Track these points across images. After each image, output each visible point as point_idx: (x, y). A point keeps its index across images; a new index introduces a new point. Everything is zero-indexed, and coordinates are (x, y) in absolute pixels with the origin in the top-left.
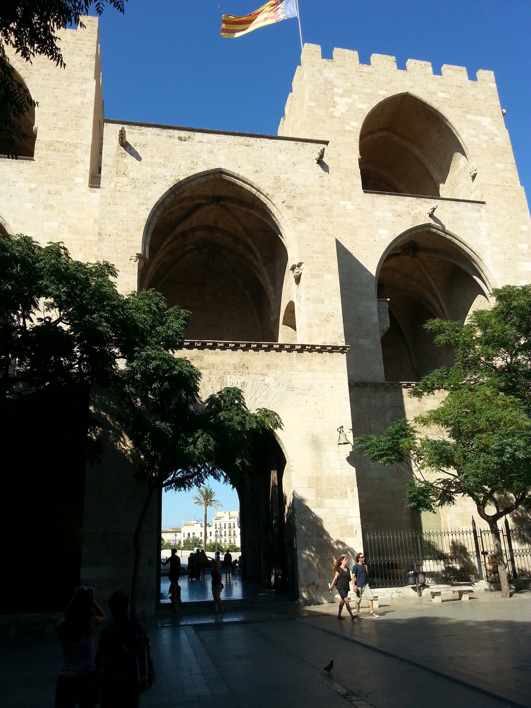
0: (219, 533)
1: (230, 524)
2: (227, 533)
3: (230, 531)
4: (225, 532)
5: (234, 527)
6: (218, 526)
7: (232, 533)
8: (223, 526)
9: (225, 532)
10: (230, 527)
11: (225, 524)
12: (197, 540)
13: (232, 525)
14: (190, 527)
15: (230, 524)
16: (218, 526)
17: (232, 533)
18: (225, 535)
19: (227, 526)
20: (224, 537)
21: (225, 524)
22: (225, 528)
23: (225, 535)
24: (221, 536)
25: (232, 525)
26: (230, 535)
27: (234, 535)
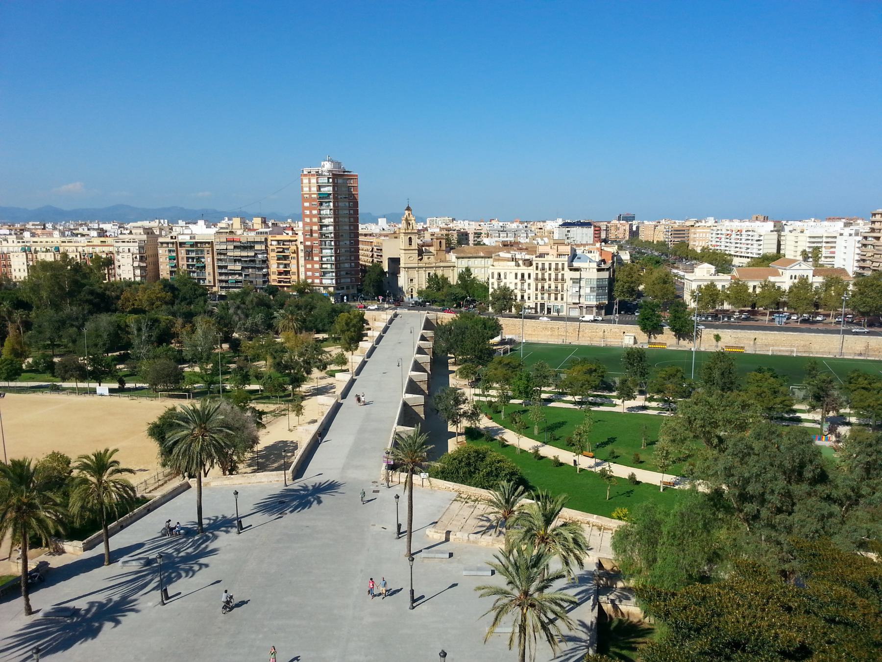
0: (540, 276)
1: (557, 264)
2: (553, 276)
3: (557, 275)
4: (550, 274)
5: (563, 269)
6: (540, 266)
7: (560, 277)
8: (547, 266)
9: (550, 274)
10: (557, 269)
11: (550, 264)
12: (506, 289)
13: (560, 266)
14: (502, 263)
15: (557, 264)
16: (540, 266)
17: (560, 277)
18: (550, 279)
19: (553, 266)
20: (548, 282)
21: (550, 264)
22: (550, 269)
23: (550, 279)
24: (543, 279)
25: (560, 266)
26: (556, 279)
27: (563, 279)
